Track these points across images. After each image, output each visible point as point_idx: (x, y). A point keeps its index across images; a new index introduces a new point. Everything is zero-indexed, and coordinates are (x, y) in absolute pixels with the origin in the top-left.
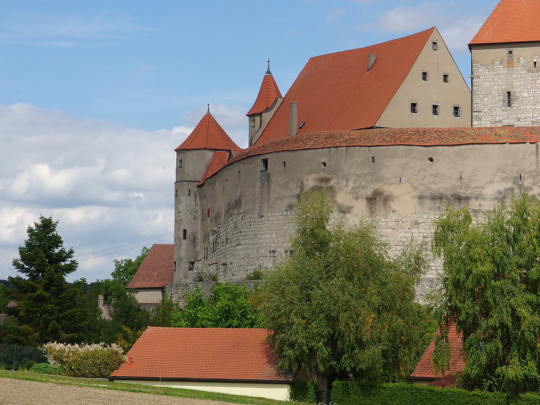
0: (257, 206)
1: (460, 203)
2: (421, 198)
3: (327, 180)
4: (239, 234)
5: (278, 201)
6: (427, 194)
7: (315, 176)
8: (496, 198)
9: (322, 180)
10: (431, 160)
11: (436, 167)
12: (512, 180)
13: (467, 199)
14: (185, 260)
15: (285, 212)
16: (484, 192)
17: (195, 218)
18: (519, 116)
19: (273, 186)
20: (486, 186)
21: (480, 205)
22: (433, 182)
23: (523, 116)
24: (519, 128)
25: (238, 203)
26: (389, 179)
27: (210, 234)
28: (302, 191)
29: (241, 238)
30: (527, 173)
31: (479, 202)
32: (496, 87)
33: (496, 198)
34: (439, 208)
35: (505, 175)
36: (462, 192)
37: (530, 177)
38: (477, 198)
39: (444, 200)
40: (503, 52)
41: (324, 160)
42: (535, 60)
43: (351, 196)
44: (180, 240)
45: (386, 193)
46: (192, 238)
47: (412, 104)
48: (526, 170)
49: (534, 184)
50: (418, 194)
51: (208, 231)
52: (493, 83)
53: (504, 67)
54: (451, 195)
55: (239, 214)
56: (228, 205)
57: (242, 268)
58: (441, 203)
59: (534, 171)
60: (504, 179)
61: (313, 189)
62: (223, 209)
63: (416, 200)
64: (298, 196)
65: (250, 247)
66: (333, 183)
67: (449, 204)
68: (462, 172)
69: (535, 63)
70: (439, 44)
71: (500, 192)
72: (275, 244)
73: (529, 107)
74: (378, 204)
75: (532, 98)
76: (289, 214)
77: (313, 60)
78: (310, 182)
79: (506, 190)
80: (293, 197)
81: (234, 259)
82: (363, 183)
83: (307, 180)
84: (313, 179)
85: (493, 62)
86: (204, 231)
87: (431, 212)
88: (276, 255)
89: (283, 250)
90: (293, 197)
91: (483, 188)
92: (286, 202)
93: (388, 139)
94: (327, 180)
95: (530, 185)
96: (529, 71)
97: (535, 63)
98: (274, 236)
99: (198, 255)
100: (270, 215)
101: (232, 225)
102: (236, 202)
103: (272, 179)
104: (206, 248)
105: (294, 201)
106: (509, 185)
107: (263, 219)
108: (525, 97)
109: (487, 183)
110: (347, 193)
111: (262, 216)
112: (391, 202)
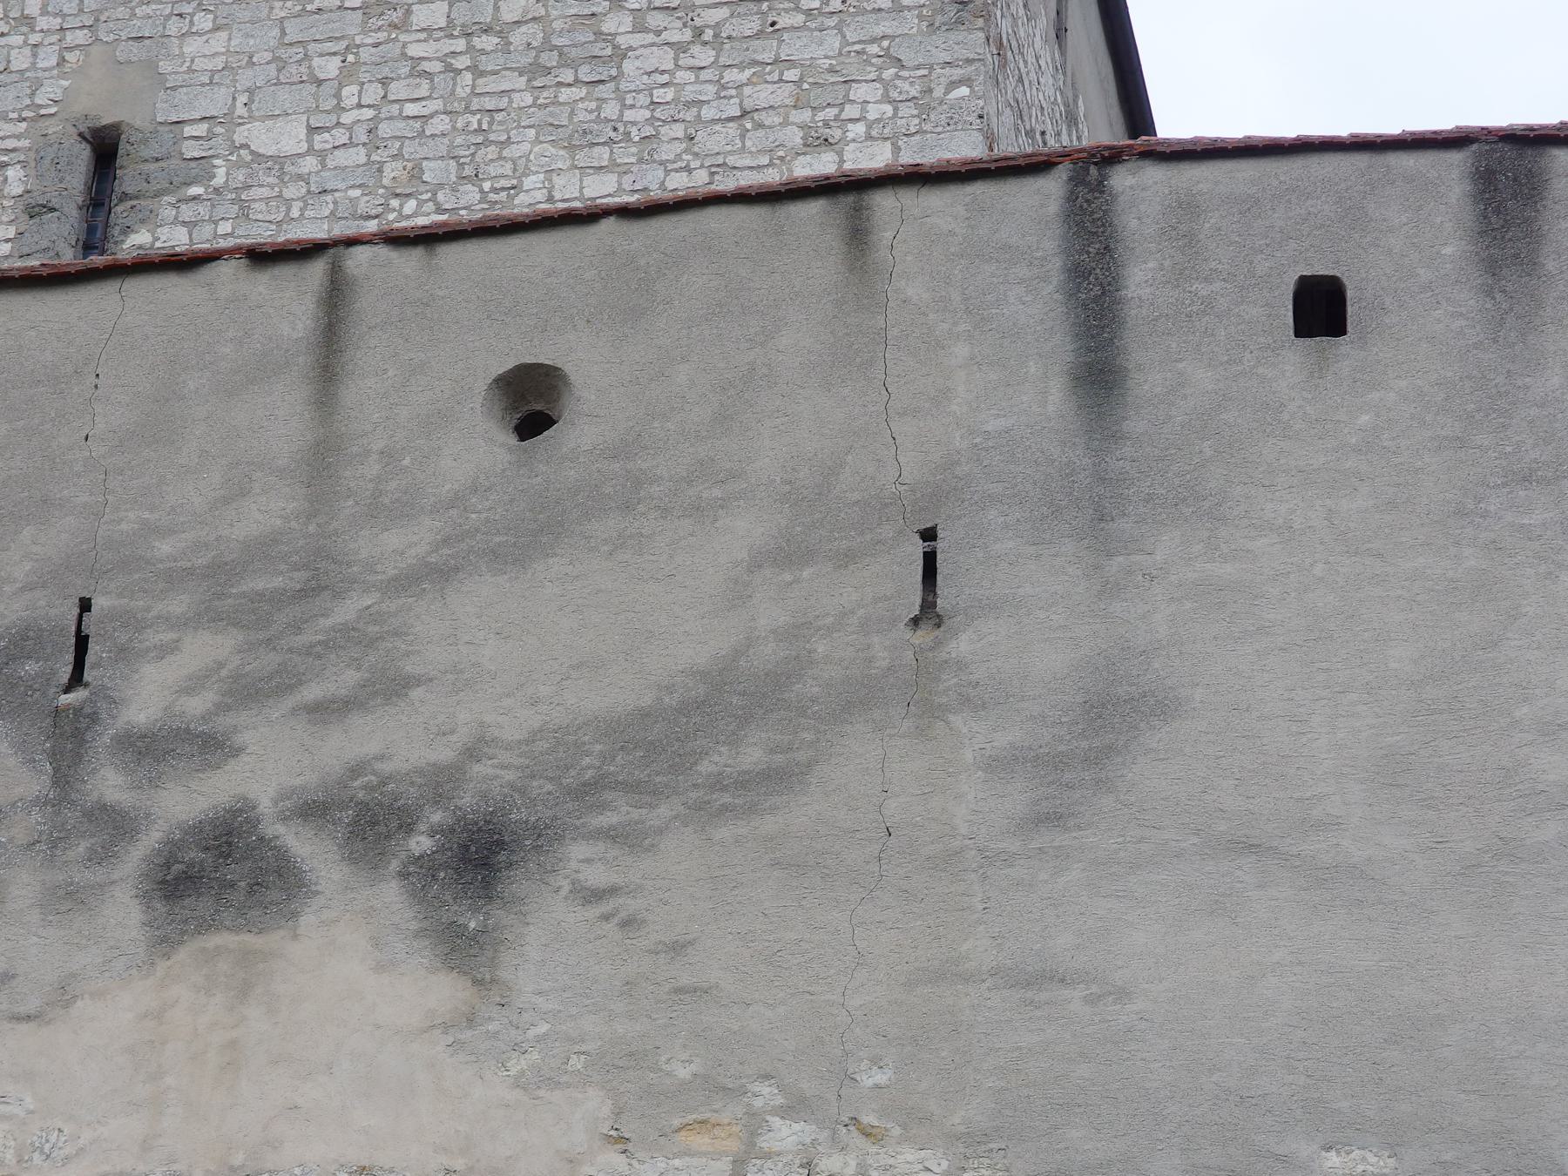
30: (175, 578)
37: (209, 617)
48: (164, 548)
59: (262, 550)
75: (358, 156)
95: (197, 705)
108: (279, 160)
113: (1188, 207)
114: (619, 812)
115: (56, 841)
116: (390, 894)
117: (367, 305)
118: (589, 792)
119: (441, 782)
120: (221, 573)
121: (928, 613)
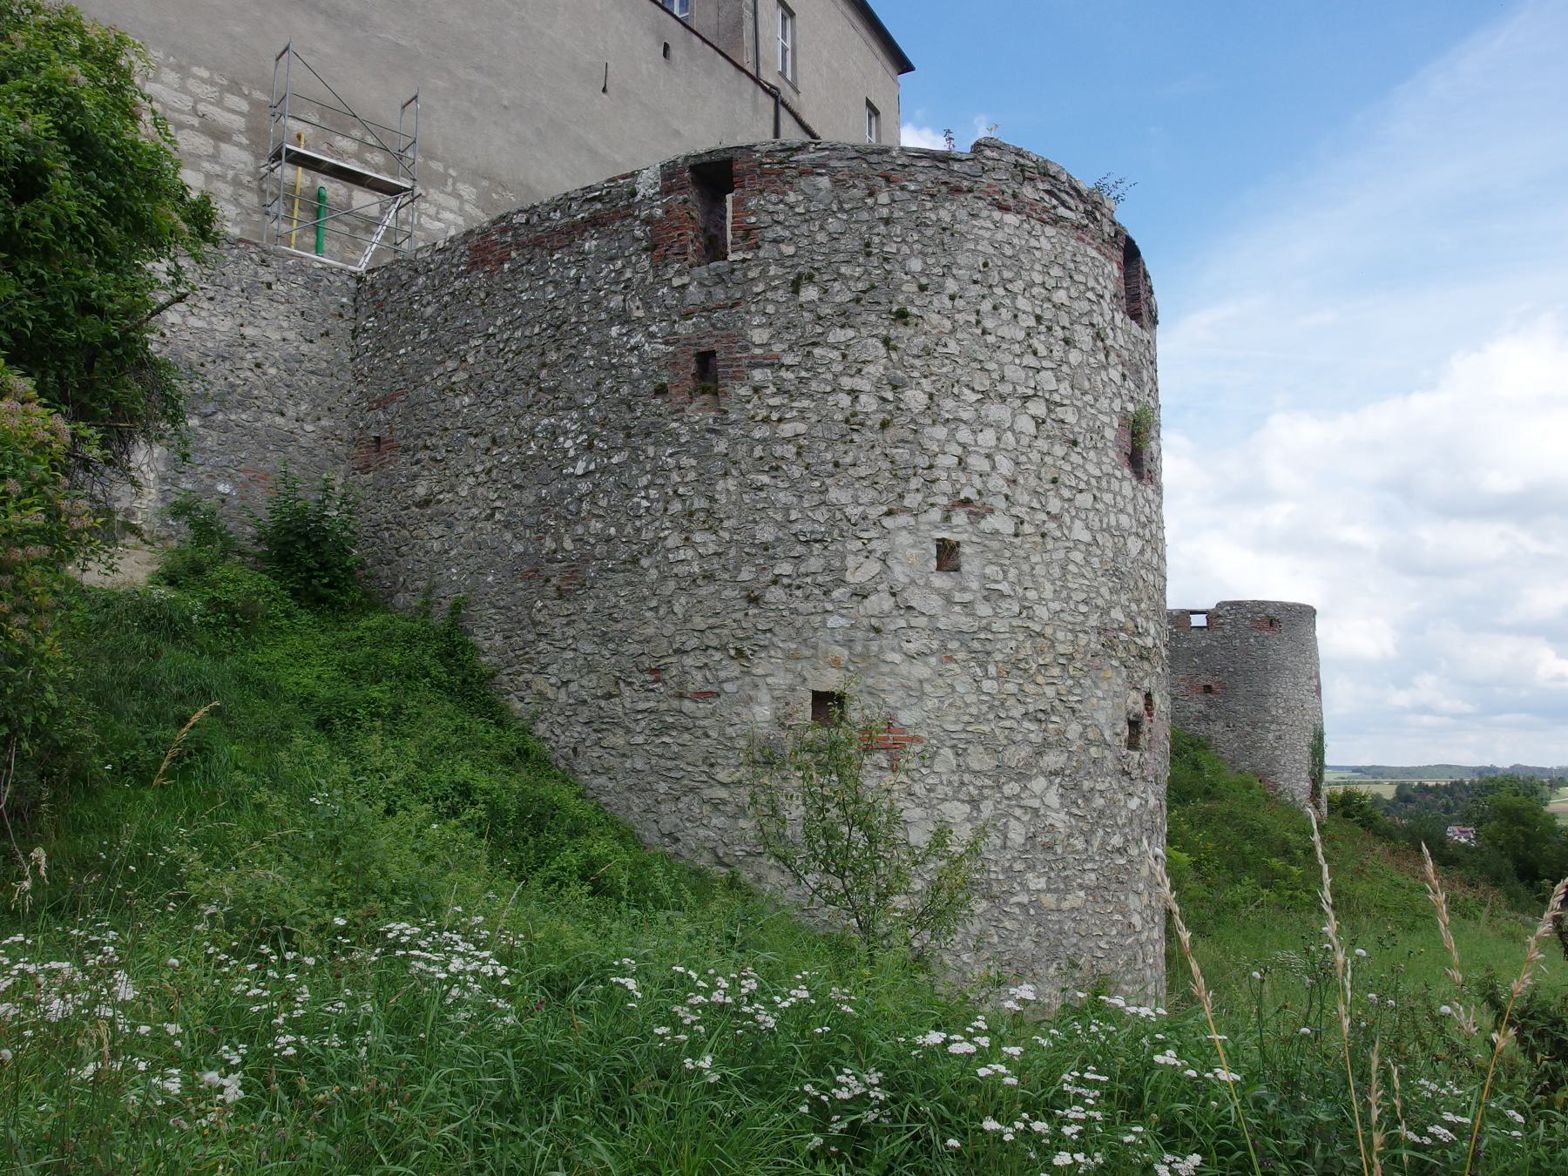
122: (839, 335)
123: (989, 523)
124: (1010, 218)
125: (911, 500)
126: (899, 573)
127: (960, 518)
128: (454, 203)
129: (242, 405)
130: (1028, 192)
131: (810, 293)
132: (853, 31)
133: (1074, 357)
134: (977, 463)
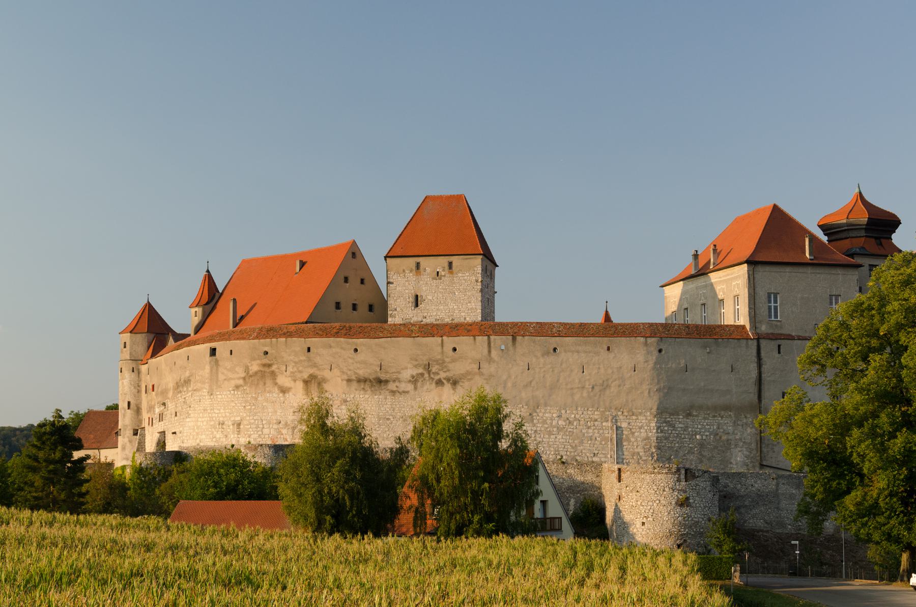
0: (207, 386)
1: (380, 385)
2: (349, 381)
3: (270, 366)
4: (188, 409)
5: (226, 382)
6: (354, 378)
7: (259, 362)
8: (410, 381)
9: (264, 365)
10: (356, 350)
11: (360, 356)
12: (423, 367)
13: (387, 382)
14: (129, 427)
15: (232, 392)
16: (400, 376)
17: (138, 392)
18: (426, 314)
19: (221, 369)
20: (402, 372)
21: (397, 387)
22: (358, 368)
23: (429, 314)
24: (427, 325)
25: (187, 382)
26: (322, 365)
27: (156, 407)
28: (248, 373)
29: (190, 412)
30: (434, 361)
31: (397, 384)
32: (407, 291)
33: (410, 381)
34: (363, 389)
35: (417, 363)
36: (383, 376)
37: (437, 364)
38: (394, 381)
39: (367, 383)
40: (412, 262)
41: (266, 349)
42: (438, 270)
43: (290, 379)
44: (125, 410)
45: (319, 377)
46: (136, 408)
47: (336, 303)
49: (439, 370)
50: (346, 377)
51: (153, 403)
52: (404, 288)
53: (413, 275)
54: (374, 379)
55: (188, 391)
56: (177, 383)
57: (191, 437)
58: (365, 385)
59: (440, 359)
60: (416, 366)
61: (256, 373)
62: (171, 385)
63: (345, 382)
64: (244, 379)
65: (200, 419)
66: (274, 368)
67: (372, 386)
68: (382, 360)
69: (438, 272)
70: (357, 254)
71: (413, 377)
72: (223, 417)
73: (433, 307)
74: (313, 385)
76: (236, 393)
77: (244, 261)
78: (255, 367)
79: (418, 374)
80: (239, 379)
81: (183, 429)
82: (300, 368)
83: (252, 365)
84: (258, 365)
85: (404, 271)
86: (148, 403)
87: (357, 392)
88: (224, 427)
89: (230, 423)
90: (239, 379)
91: (399, 373)
92: (233, 383)
93: (320, 333)
94: (270, 366)
96: (434, 279)
97: (438, 272)
98: (222, 411)
99: (141, 423)
100: (218, 393)
101: (181, 400)
102: (185, 381)
103: (220, 363)
104: (151, 419)
105: (241, 382)
106: (421, 371)
107: (212, 397)
109: (402, 369)
110: (286, 376)
111: (211, 394)
112: (324, 384)
113: (495, 339)
114: (463, 380)
115: (429, 380)
116: (449, 385)
117: (444, 341)
118: (460, 379)
119: (452, 377)
120: (438, 361)
121: (479, 368)
122: (631, 494)
123: (649, 519)
124: (653, 475)
125: (639, 517)
126: (637, 526)
127: (645, 519)
128: (644, 418)
129: (586, 491)
130: (656, 470)
131: (628, 488)
132: (818, 276)
133: (665, 493)
134: (647, 511)
